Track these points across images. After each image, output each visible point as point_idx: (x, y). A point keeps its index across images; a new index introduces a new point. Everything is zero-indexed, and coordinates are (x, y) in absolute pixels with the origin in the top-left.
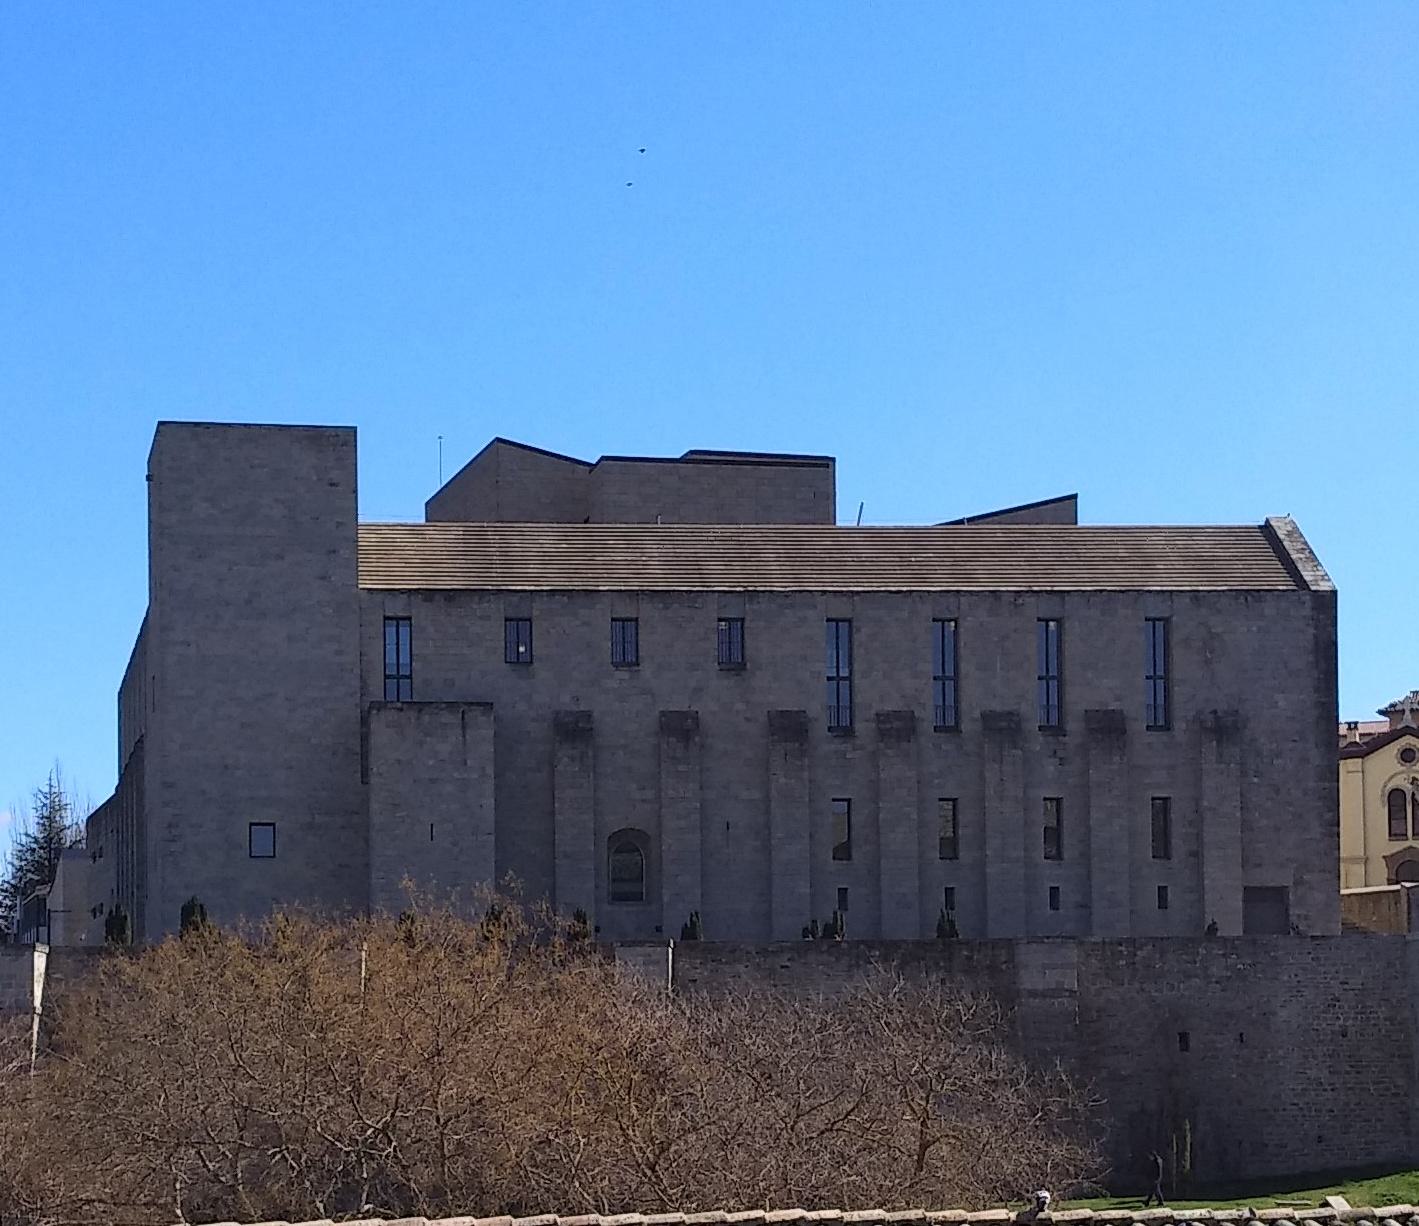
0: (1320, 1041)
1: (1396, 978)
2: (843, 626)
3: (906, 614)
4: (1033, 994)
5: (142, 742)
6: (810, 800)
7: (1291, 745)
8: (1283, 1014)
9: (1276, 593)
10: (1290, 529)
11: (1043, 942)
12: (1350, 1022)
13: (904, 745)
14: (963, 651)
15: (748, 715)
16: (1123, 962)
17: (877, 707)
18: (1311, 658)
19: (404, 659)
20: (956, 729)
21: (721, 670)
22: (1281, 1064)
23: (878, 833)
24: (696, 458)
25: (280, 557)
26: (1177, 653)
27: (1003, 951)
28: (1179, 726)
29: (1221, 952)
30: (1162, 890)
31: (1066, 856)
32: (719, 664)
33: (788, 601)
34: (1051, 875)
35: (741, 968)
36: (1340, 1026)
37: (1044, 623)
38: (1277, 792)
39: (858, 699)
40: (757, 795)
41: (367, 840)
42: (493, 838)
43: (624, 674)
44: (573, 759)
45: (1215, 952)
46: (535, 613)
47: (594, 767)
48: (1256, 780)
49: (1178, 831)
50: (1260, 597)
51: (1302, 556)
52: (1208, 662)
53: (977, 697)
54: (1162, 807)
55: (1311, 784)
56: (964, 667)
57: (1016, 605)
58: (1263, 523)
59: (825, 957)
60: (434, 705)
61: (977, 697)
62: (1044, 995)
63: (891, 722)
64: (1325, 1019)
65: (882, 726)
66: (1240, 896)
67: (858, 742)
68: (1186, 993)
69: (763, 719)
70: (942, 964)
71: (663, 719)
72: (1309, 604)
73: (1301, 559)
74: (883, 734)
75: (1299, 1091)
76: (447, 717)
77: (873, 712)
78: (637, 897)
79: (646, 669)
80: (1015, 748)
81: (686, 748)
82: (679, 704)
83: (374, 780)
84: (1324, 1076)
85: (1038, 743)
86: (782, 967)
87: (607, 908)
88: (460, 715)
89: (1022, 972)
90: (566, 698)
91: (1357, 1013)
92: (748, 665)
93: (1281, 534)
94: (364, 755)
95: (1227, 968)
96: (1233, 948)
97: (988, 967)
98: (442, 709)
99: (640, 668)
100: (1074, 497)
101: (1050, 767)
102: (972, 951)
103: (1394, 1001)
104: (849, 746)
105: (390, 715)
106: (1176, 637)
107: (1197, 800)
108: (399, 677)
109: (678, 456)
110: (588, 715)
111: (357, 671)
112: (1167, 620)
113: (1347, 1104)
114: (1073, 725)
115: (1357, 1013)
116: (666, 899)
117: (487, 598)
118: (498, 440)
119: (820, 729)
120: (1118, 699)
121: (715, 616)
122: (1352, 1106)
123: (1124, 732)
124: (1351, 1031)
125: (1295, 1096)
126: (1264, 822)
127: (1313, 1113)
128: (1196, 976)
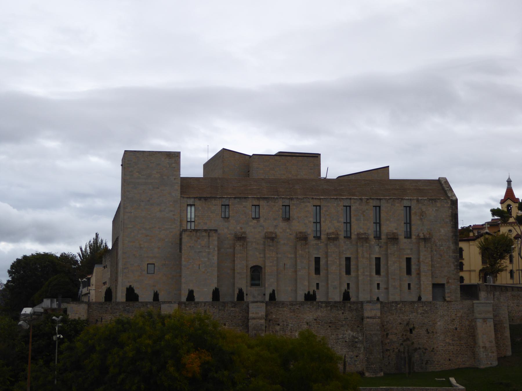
0: (449, 331)
1: (471, 313)
2: (318, 208)
3: (335, 205)
4: (368, 318)
5: (118, 239)
6: (308, 258)
7: (445, 243)
8: (439, 323)
9: (440, 200)
10: (445, 181)
11: (371, 303)
12: (458, 326)
13: (335, 242)
14: (352, 215)
15: (291, 233)
16: (394, 308)
17: (327, 231)
18: (451, 218)
19: (193, 216)
20: (350, 238)
21: (283, 220)
22: (438, 338)
23: (328, 267)
24: (281, 154)
25: (158, 188)
26: (413, 217)
27: (360, 305)
28: (414, 237)
29: (421, 306)
30: (409, 285)
31: (382, 274)
32: (282, 218)
34: (377, 279)
35: (285, 309)
36: (455, 327)
37: (375, 207)
38: (441, 256)
39: (322, 229)
40: (293, 256)
41: (181, 269)
42: (217, 268)
43: (255, 221)
44: (240, 245)
45: (420, 305)
46: (230, 204)
47: (246, 247)
48: (435, 253)
49: (414, 267)
50: (436, 201)
51: (448, 189)
52: (421, 219)
53: (356, 228)
54: (409, 260)
55: (451, 254)
56: (353, 220)
57: (367, 203)
58: (438, 179)
59: (309, 306)
60: (201, 230)
61: (356, 228)
62: (371, 318)
63: (331, 236)
64: (451, 325)
65: (329, 236)
66: (431, 286)
68: (412, 317)
69: (294, 234)
70: (342, 308)
71: (266, 234)
72: (450, 203)
73: (448, 190)
74: (329, 239)
75: (444, 346)
76: (204, 234)
77: (326, 232)
78: (258, 285)
79: (262, 220)
80: (367, 243)
82: (271, 229)
83: (183, 252)
84: (451, 342)
85: (373, 242)
86: (297, 309)
87: (249, 288)
88: (208, 233)
89: (365, 311)
90: (239, 228)
91: (460, 323)
92: (291, 219)
93: (443, 182)
94: (181, 244)
95: (423, 310)
96: (425, 304)
97: (355, 309)
98: (203, 232)
99: (260, 219)
100: (388, 167)
101: (377, 248)
103: (470, 320)
104: (319, 242)
105: (188, 233)
106: (413, 212)
107: (419, 259)
108: (191, 222)
109: (274, 154)
111: (179, 220)
112: (410, 207)
113: (457, 350)
114: (383, 237)
115: (460, 323)
116: (266, 286)
118: (224, 149)
119: (311, 238)
120: (396, 229)
121: (281, 204)
122: (458, 350)
123: (397, 239)
124: (458, 329)
125: (443, 347)
126: (438, 265)
127: (447, 352)
128: (414, 312)
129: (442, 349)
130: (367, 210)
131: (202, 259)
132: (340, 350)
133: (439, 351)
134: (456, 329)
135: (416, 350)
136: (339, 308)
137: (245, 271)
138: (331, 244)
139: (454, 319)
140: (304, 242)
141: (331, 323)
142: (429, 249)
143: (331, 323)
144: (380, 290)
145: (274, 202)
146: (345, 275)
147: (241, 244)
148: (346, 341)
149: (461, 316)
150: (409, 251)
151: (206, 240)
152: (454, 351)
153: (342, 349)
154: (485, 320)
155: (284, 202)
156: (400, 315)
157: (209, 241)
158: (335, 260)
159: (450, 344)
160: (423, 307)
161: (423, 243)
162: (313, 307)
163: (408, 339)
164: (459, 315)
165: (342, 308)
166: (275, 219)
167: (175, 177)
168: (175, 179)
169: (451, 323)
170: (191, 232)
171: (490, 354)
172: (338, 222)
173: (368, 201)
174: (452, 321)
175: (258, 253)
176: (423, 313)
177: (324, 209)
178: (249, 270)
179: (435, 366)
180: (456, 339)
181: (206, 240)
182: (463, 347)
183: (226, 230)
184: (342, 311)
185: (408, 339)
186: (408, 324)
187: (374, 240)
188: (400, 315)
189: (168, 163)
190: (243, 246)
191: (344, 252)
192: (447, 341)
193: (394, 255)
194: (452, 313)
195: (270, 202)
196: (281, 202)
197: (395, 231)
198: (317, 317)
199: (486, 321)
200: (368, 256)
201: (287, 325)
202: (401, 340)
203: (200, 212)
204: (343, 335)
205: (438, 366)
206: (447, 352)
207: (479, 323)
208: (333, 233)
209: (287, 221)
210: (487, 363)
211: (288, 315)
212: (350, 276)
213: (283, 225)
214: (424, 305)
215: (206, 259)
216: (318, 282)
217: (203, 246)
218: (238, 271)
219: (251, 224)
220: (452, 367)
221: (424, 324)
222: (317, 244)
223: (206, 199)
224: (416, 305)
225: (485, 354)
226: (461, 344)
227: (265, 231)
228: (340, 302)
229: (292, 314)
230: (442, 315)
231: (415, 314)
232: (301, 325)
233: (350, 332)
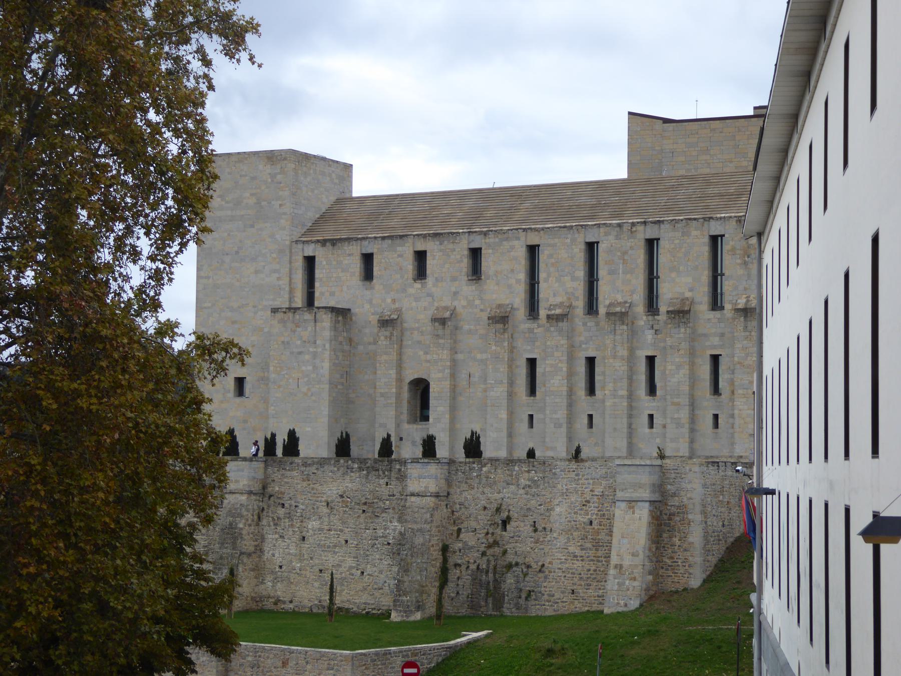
0: (577, 528)
3: (569, 241)
4: (412, 495)
8: (558, 509)
13: (560, 324)
15: (482, 307)
30: (716, 417)
33: (506, 235)
34: (647, 405)
35: (295, 473)
43: (418, 285)
44: (386, 337)
52: (745, 263)
57: (632, 232)
59: (332, 468)
64: (581, 515)
67: (540, 322)
68: (507, 495)
70: (386, 473)
77: (549, 303)
79: (430, 280)
80: (623, 324)
81: (444, 328)
82: (447, 302)
84: (578, 552)
87: (406, 426)
90: (389, 301)
95: (529, 480)
96: (533, 466)
101: (649, 336)
102: (401, 466)
104: (535, 325)
110: (399, 311)
113: (589, 570)
117: (351, 243)
120: (691, 290)
124: (595, 523)
125: (561, 563)
128: (512, 484)
129: (560, 566)
130: (631, 248)
131: (304, 368)
132: (377, 561)
133: (554, 572)
134: (591, 523)
135: (510, 566)
136: (381, 472)
137: (394, 390)
138: (552, 329)
139: (588, 502)
140: (501, 326)
141: (365, 504)
142: (753, 333)
143: (365, 504)
144: (654, 430)
145: (453, 243)
146: (584, 397)
147: (388, 334)
148: (389, 544)
149: (601, 494)
150: (716, 340)
151: (310, 329)
152: (582, 573)
153: (381, 560)
154: (631, 503)
155: (473, 241)
156: (485, 490)
157: (315, 331)
158: (560, 365)
159: (576, 556)
160: (529, 472)
161: (742, 319)
162: (338, 470)
163: (496, 543)
164: (598, 491)
165: (386, 473)
166: (454, 279)
167: (280, 203)
168: (281, 205)
169: (581, 510)
170: (285, 313)
171: (627, 582)
172: (574, 279)
173: (634, 229)
174: (583, 505)
175: (421, 353)
176: (529, 486)
177: (546, 252)
178: (406, 388)
179: (544, 605)
180: (589, 545)
181: (310, 329)
182: (600, 564)
183: (367, 306)
184: (386, 480)
185: (496, 543)
186: (498, 510)
187: (645, 318)
188: (485, 490)
189: (270, 174)
190: (390, 339)
191: (584, 346)
192: (571, 549)
193: (678, 350)
194: (584, 486)
195: (446, 242)
196: (466, 242)
197: (688, 294)
198: (345, 492)
199: (633, 507)
200: (625, 353)
201: (296, 506)
202: (484, 545)
203: (324, 271)
204: (385, 529)
205: (550, 604)
206: (570, 575)
207: (620, 511)
208: (561, 305)
209: (477, 283)
210: (618, 603)
211: (299, 486)
212: (593, 397)
213: (468, 290)
214: (531, 469)
215: (310, 368)
216: (530, 413)
217: (305, 342)
218: (382, 391)
219: (411, 291)
220: (576, 608)
221: (529, 509)
222: (531, 331)
223: (334, 242)
224: (516, 468)
225: (616, 581)
226: (599, 557)
227: (436, 304)
228: (329, 459)
229: (305, 484)
230: (565, 491)
231: (513, 488)
232: (318, 508)
233: (396, 524)
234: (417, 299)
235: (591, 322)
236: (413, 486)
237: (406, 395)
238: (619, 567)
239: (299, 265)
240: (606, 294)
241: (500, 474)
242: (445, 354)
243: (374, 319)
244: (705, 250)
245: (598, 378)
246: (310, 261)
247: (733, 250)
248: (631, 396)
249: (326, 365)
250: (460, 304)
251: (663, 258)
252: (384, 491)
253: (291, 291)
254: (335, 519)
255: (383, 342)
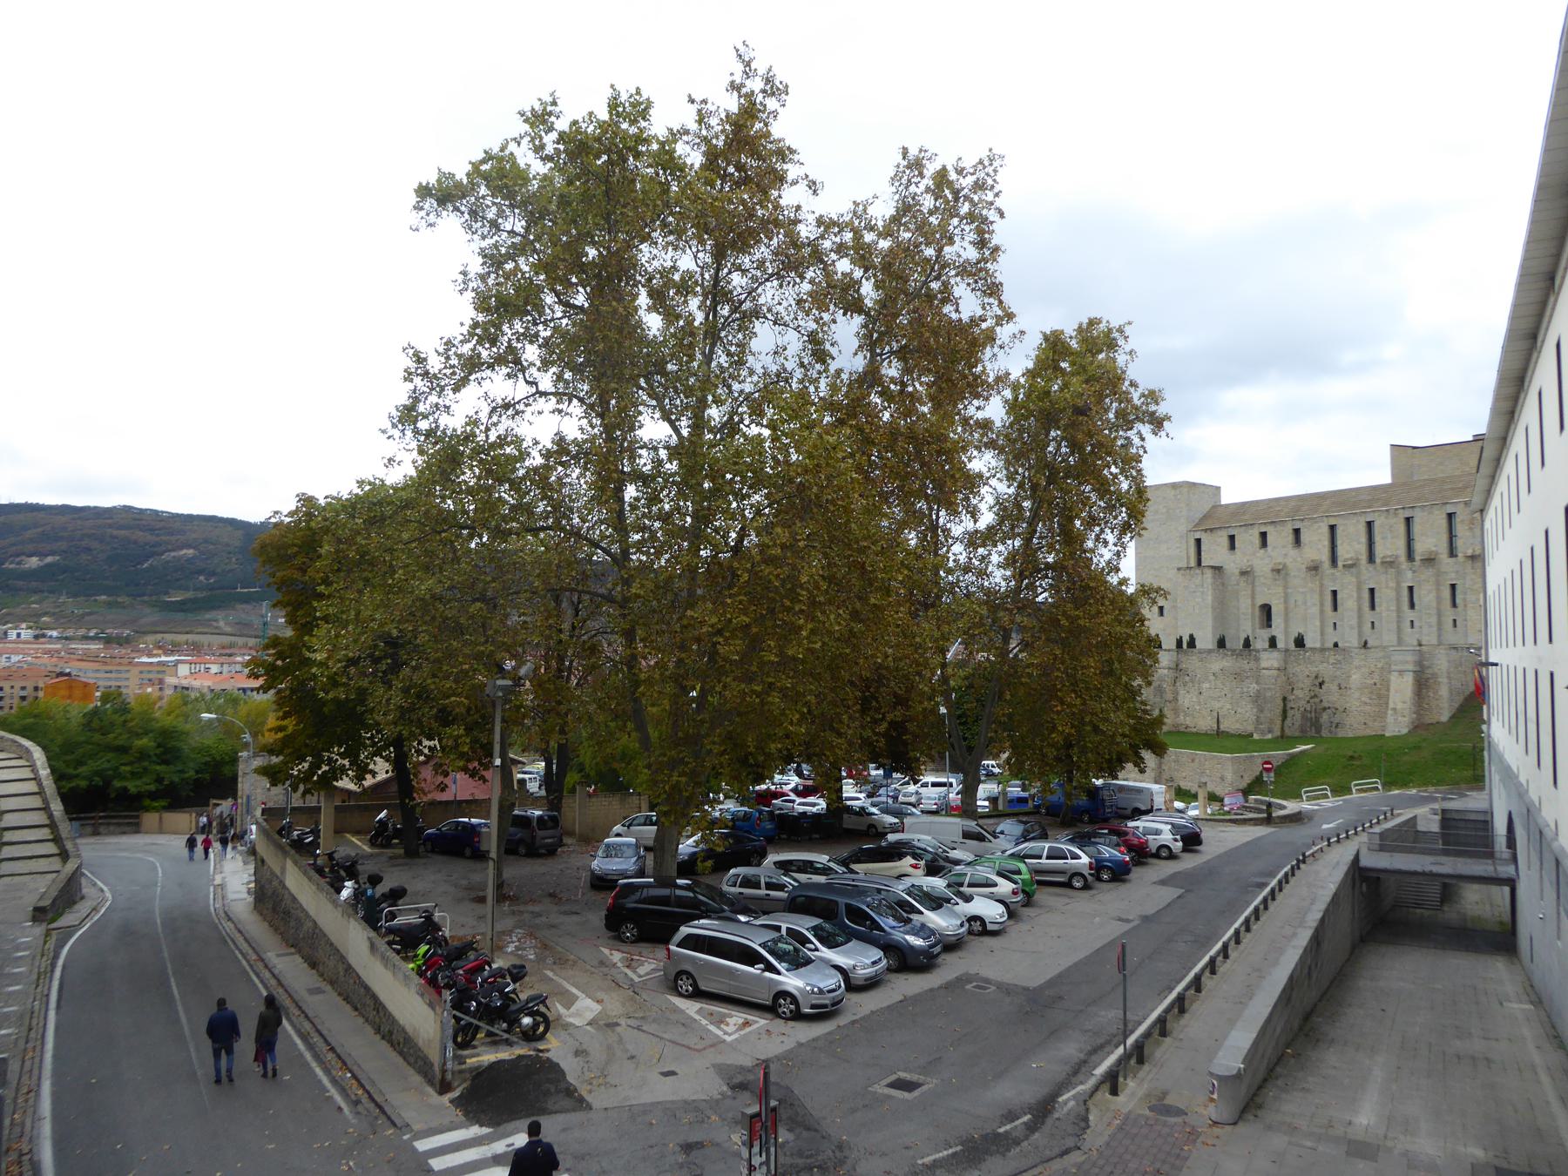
30: (1455, 621)
34: (1410, 615)
43: (1262, 551)
52: (1471, 529)
79: (1269, 548)
82: (1280, 560)
101: (1409, 574)
110: (1251, 566)
135: (1325, 709)
150: (1453, 575)
154: (1401, 672)
163: (1315, 696)
164: (1380, 665)
166: (1284, 547)
185: (1315, 696)
186: (1316, 677)
207: (1394, 677)
208: (1351, 559)
213: (1293, 552)
223: (1211, 530)
234: (1262, 559)
235: (1371, 567)
236: (1264, 664)
237: (1257, 612)
238: (1394, 709)
239: (1192, 543)
240: (1380, 551)
241: (1317, 657)
242: (1280, 590)
243: (1237, 572)
244: (1444, 523)
245: (1376, 600)
246: (1198, 541)
247: (1462, 521)
248: (1399, 610)
249: (1210, 598)
250: (1288, 561)
251: (1417, 528)
252: (1247, 667)
253: (1188, 558)
254: (1218, 683)
255: (1242, 584)
